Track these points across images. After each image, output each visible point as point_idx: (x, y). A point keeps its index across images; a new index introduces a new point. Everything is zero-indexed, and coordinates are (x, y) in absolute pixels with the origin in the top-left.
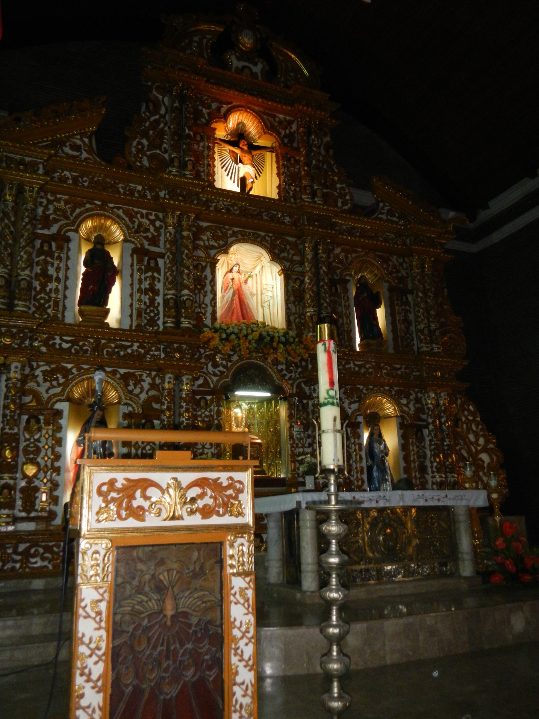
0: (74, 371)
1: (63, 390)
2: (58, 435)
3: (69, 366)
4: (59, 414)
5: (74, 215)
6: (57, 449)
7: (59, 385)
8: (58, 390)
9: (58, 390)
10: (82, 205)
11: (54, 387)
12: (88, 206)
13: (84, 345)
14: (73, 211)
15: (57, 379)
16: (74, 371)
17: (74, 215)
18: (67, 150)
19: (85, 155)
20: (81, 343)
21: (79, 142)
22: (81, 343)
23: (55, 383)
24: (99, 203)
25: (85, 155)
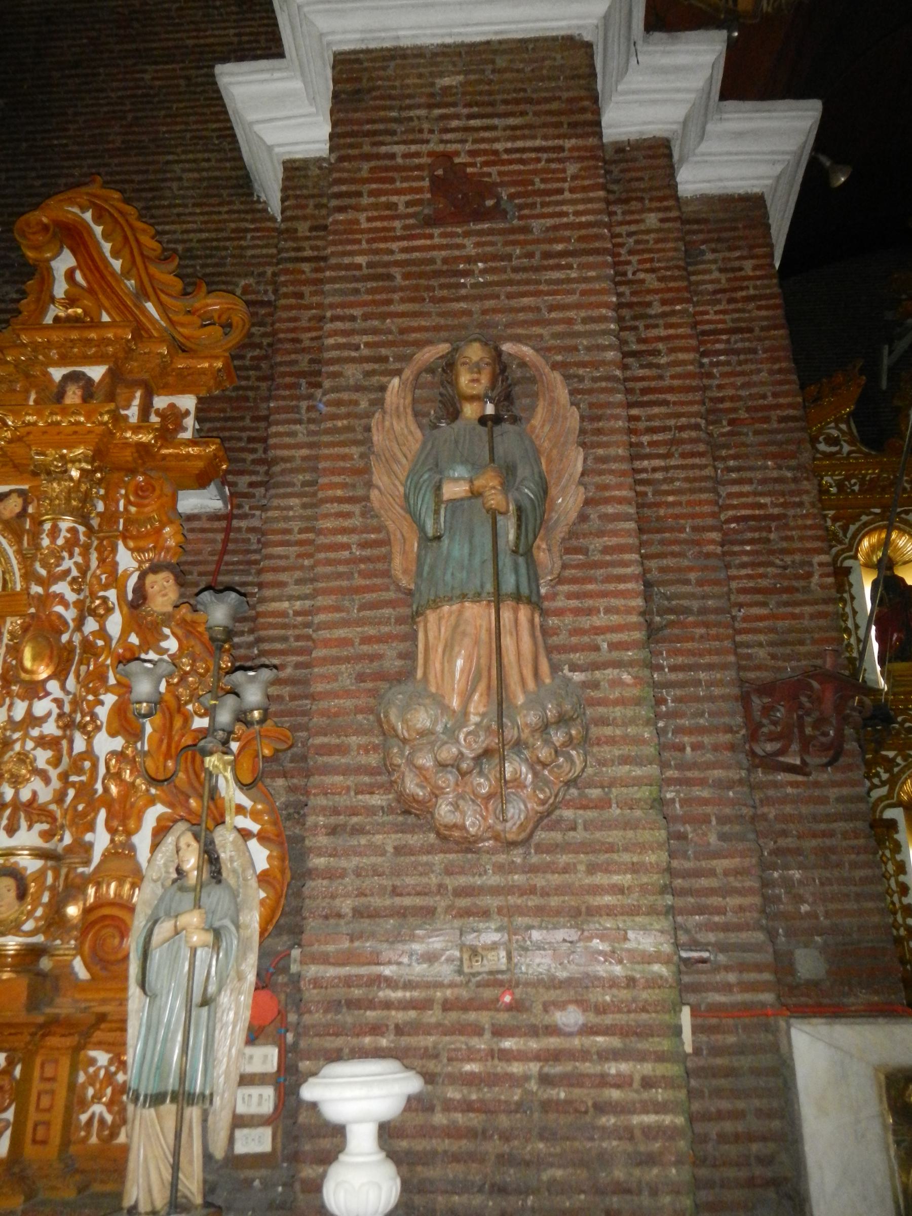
0: (899, 760)
1: (891, 790)
2: (899, 857)
3: (891, 754)
4: (892, 825)
5: (849, 535)
6: (902, 878)
7: (883, 783)
8: (884, 791)
9: (884, 791)
10: (856, 518)
11: (876, 787)
12: (864, 518)
13: (904, 721)
14: (845, 529)
15: (878, 775)
16: (899, 760)
17: (849, 535)
18: (822, 447)
19: (846, 448)
20: (900, 719)
21: (835, 433)
22: (900, 719)
23: (876, 781)
24: (878, 511)
25: (846, 448)
